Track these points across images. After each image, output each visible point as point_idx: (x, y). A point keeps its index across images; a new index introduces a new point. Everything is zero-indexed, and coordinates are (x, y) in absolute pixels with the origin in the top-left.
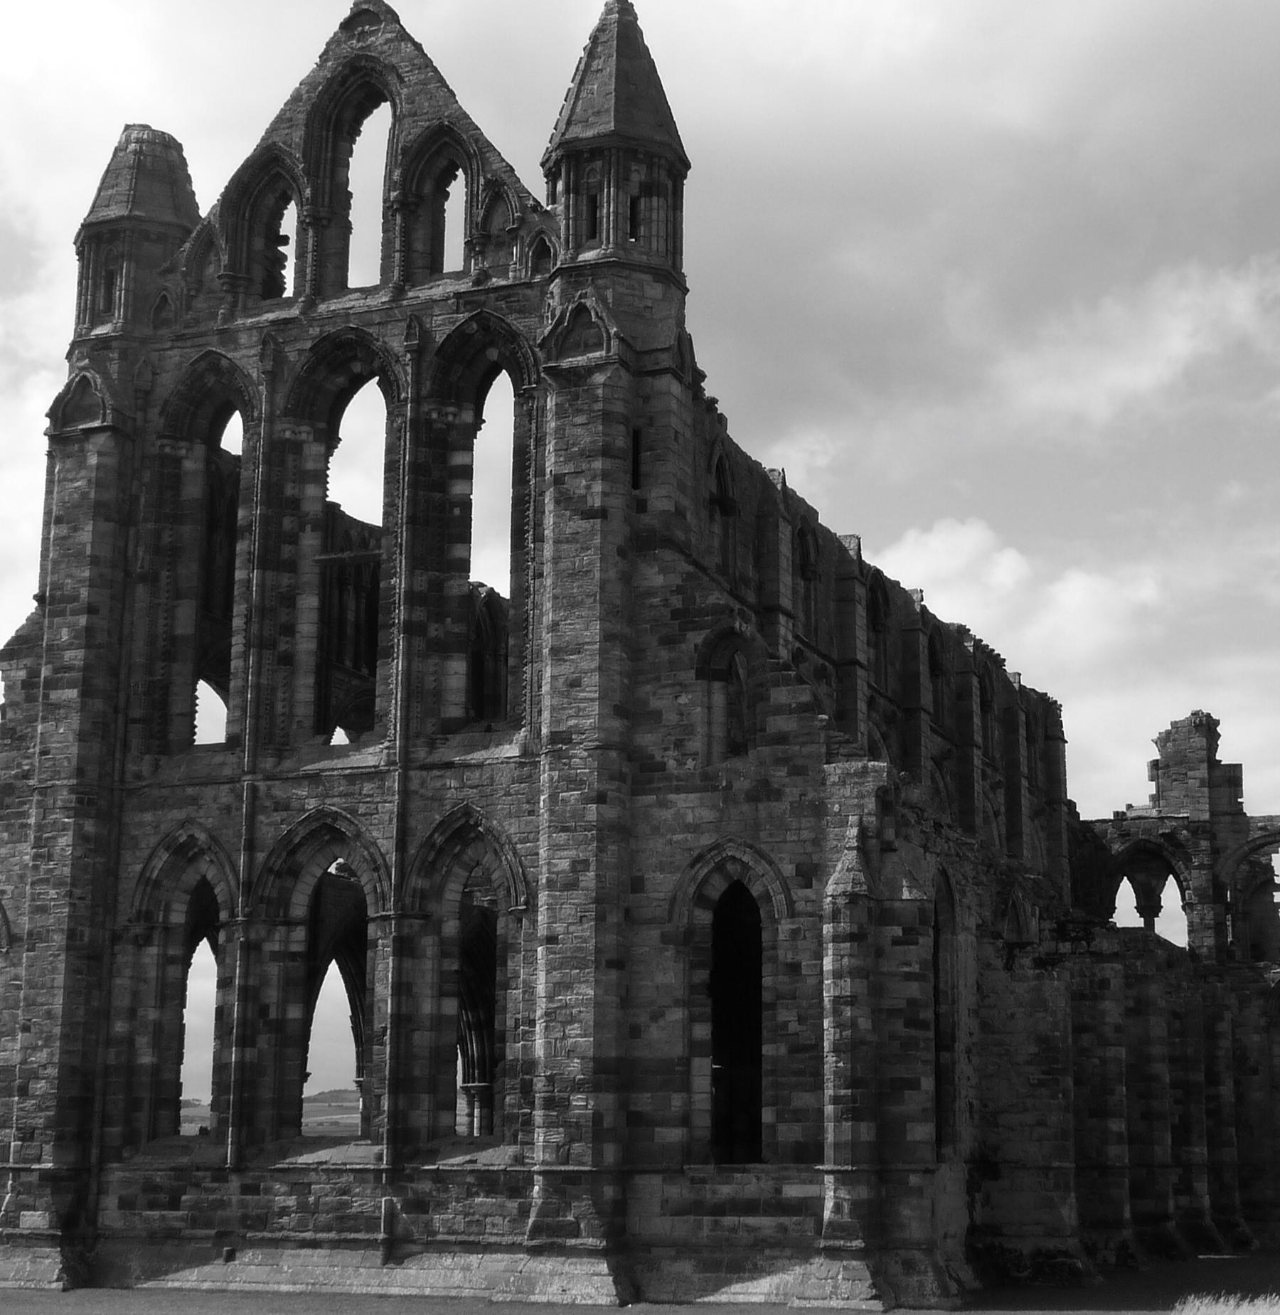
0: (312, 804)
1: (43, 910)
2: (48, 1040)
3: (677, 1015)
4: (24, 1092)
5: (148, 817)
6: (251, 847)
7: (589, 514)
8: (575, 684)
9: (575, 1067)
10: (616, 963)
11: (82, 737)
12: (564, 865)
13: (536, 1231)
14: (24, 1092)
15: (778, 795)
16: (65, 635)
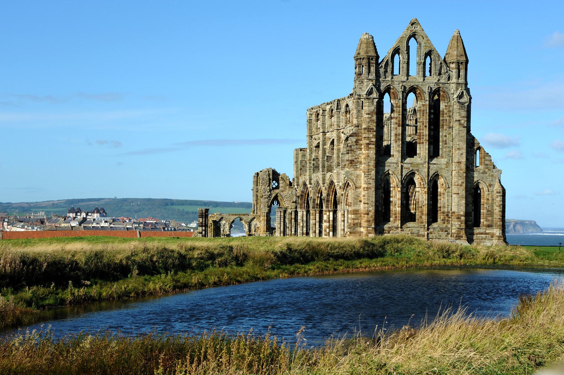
0: (411, 169)
1: (370, 184)
2: (372, 206)
3: (471, 205)
4: (368, 214)
5: (381, 168)
6: (402, 175)
7: (464, 127)
8: (462, 154)
9: (462, 213)
10: (466, 198)
11: (376, 154)
12: (460, 182)
13: (456, 237)
14: (368, 214)
15: (486, 173)
16: (371, 136)
